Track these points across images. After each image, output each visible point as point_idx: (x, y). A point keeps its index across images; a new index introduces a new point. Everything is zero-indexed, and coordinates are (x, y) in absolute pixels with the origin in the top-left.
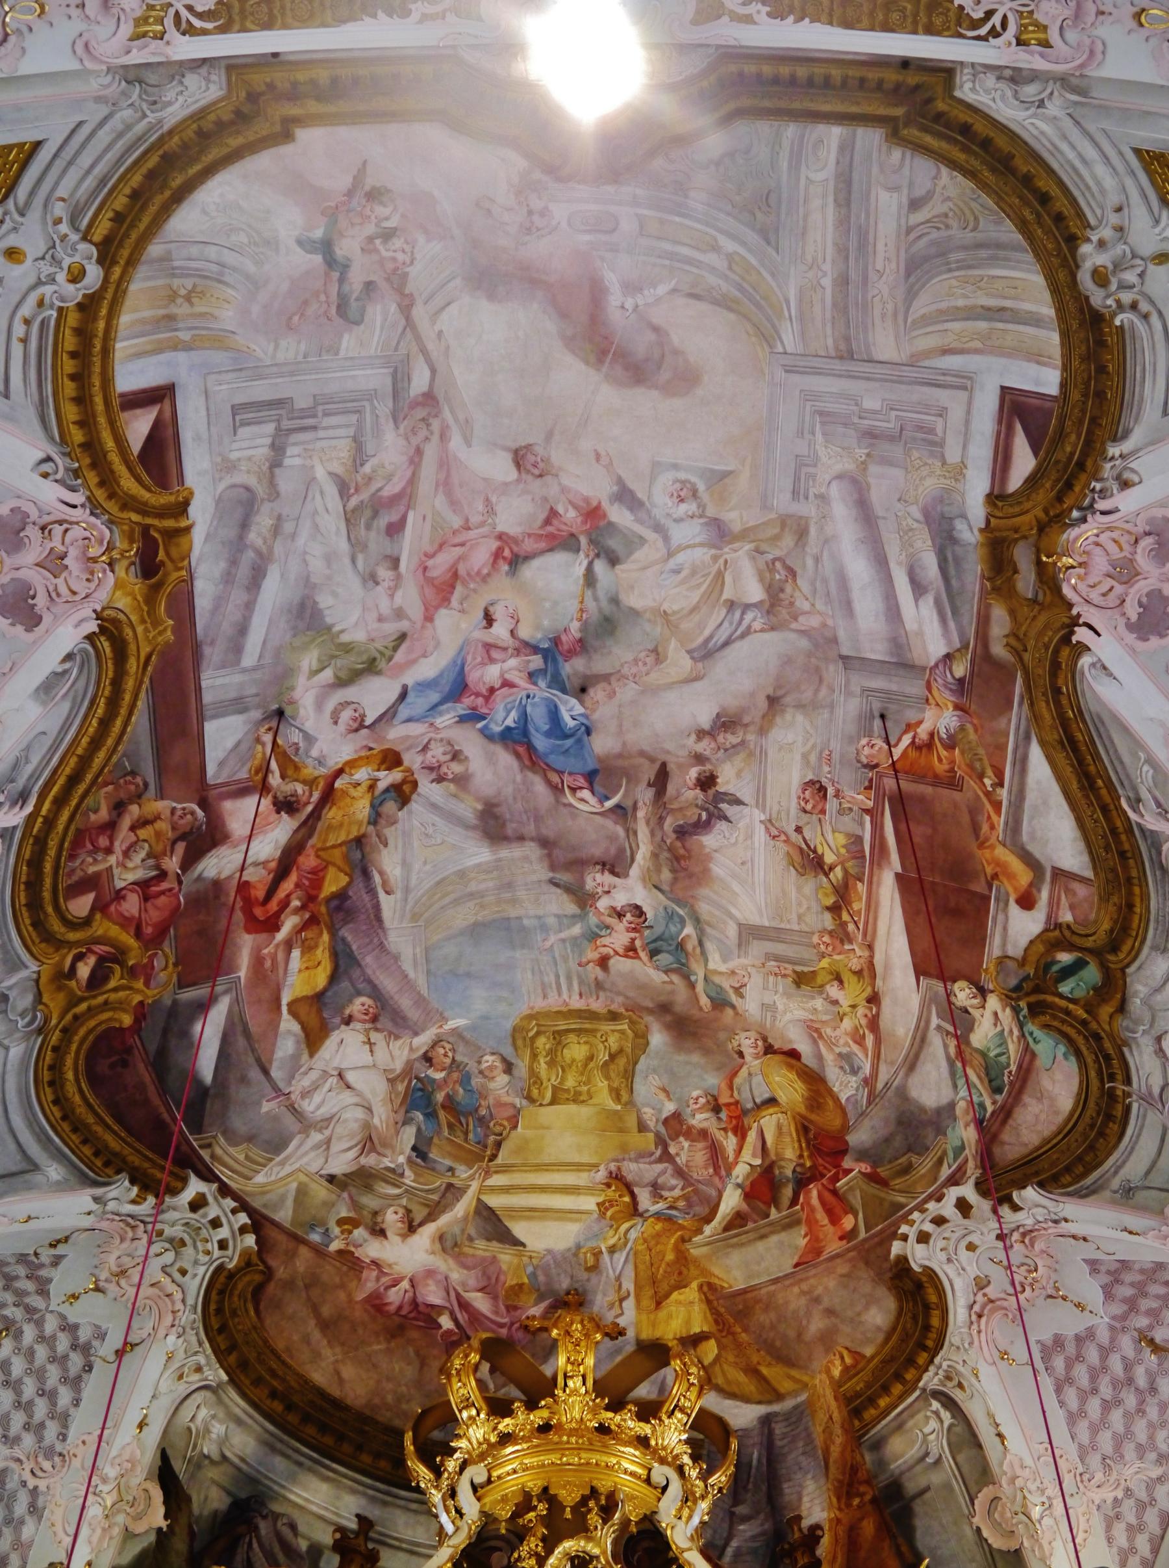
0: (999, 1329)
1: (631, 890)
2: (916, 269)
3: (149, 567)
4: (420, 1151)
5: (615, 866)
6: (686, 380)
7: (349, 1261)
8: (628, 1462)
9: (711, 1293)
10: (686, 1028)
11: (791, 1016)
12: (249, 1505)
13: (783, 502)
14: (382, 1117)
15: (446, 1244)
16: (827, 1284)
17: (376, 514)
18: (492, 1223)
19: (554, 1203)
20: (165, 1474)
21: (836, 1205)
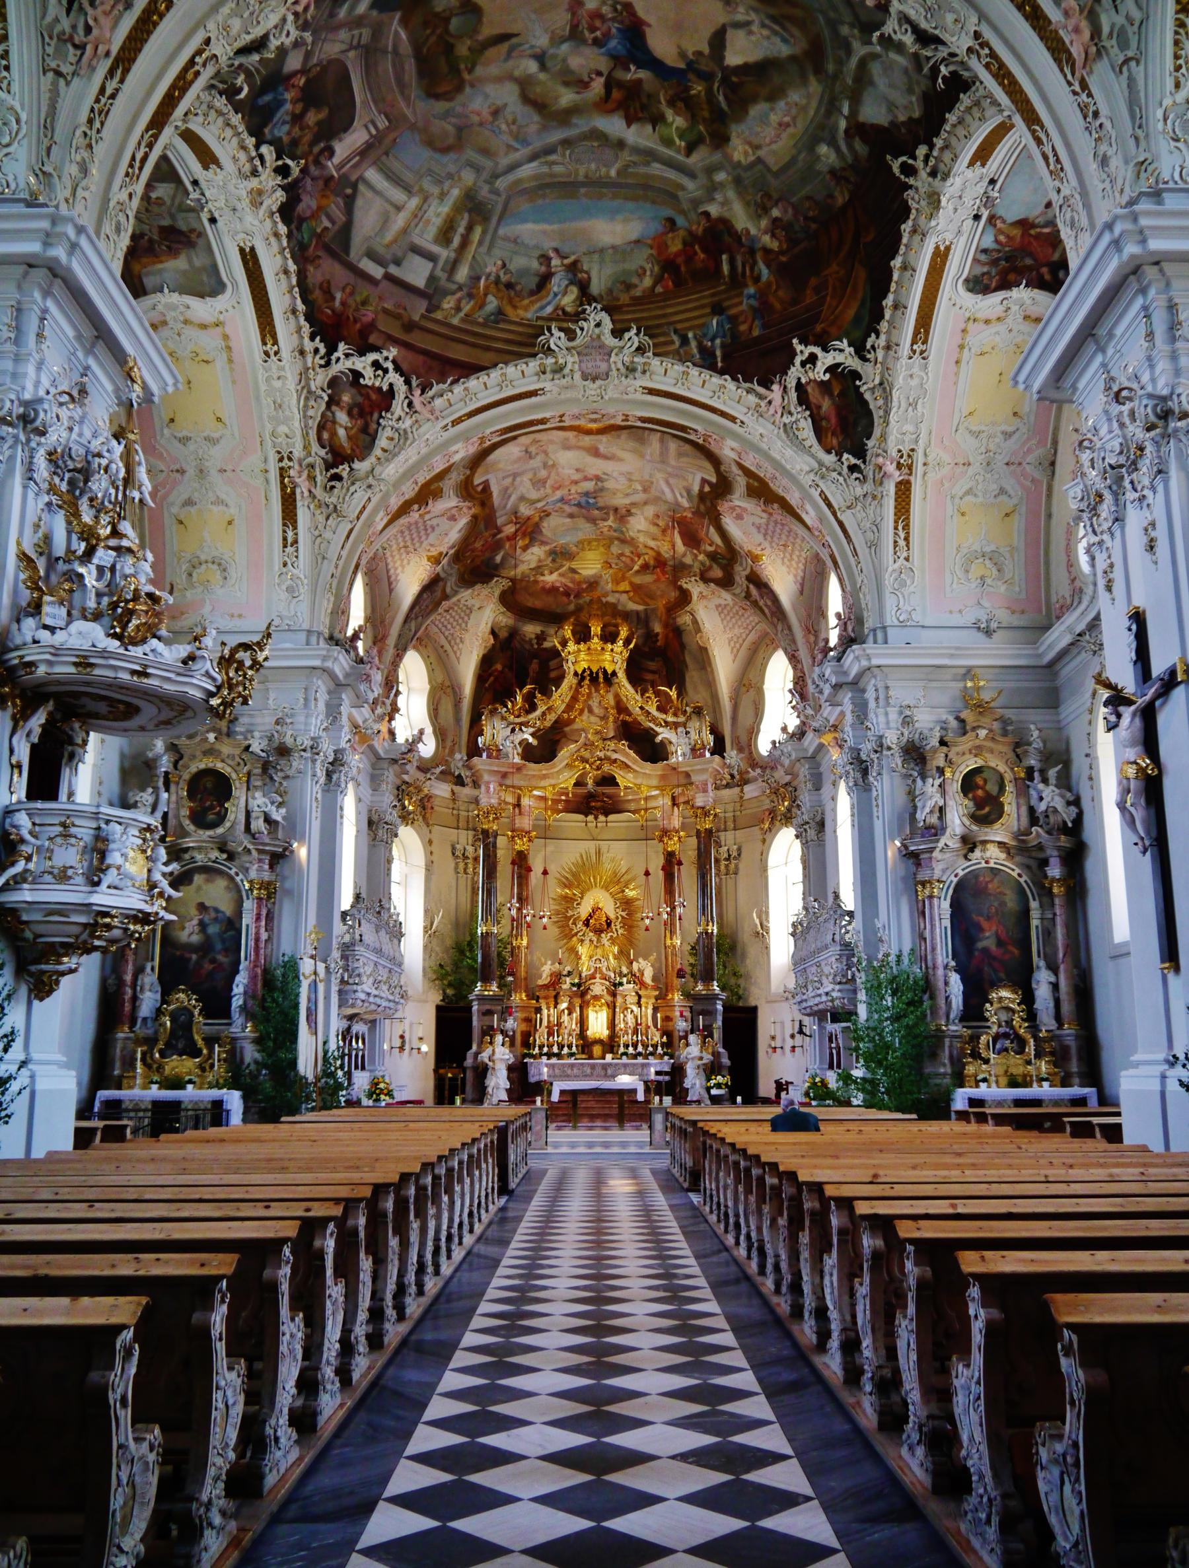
0: (705, 602)
1: (609, 523)
2: (680, 455)
3: (483, 504)
4: (554, 561)
5: (605, 520)
6: (621, 460)
7: (536, 582)
8: (607, 656)
9: (631, 584)
10: (623, 541)
11: (652, 544)
12: (513, 633)
13: (647, 477)
14: (543, 556)
15: (561, 575)
16: (663, 586)
17: (538, 483)
18: (574, 571)
19: (590, 565)
20: (493, 632)
21: (664, 573)
